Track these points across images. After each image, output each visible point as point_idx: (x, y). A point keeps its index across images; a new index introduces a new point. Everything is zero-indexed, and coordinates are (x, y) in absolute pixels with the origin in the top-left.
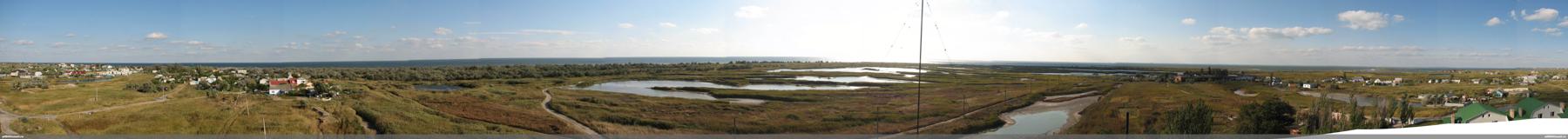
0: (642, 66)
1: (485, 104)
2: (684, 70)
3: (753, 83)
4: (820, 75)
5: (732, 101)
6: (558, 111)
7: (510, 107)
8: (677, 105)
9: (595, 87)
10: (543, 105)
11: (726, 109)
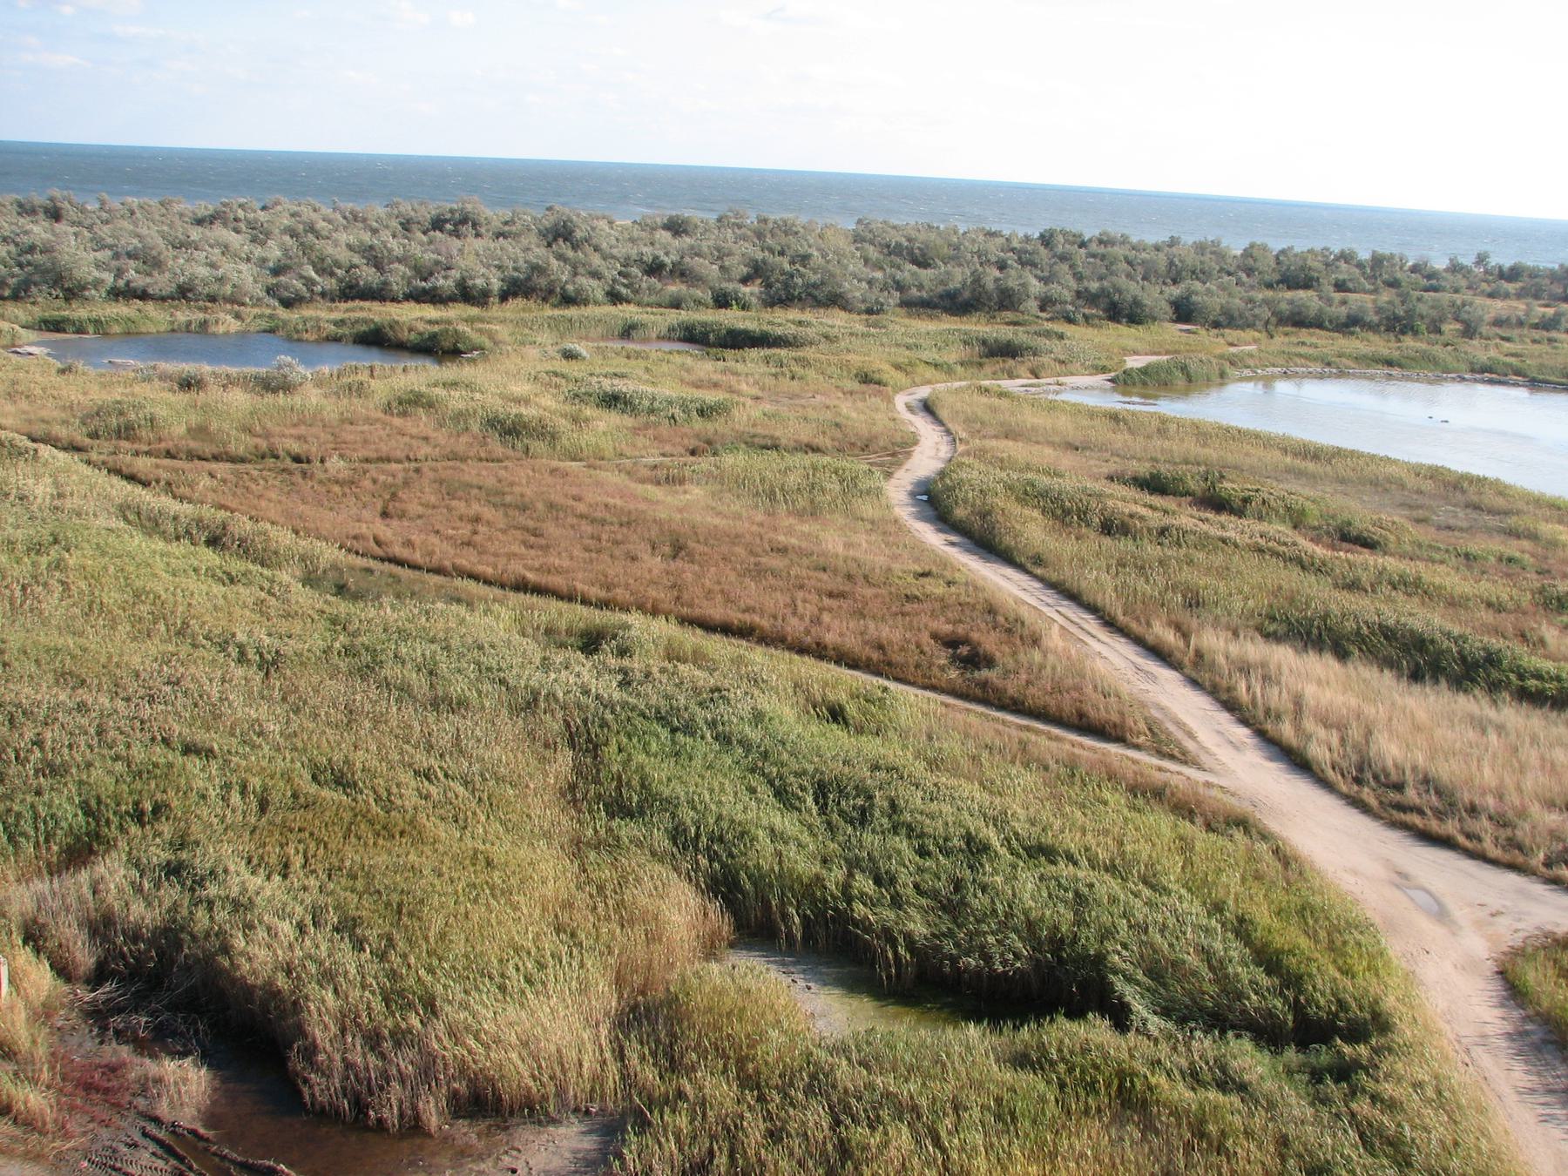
1: (527, 476)
6: (987, 544)
7: (692, 503)
9: (1235, 406)
10: (898, 491)
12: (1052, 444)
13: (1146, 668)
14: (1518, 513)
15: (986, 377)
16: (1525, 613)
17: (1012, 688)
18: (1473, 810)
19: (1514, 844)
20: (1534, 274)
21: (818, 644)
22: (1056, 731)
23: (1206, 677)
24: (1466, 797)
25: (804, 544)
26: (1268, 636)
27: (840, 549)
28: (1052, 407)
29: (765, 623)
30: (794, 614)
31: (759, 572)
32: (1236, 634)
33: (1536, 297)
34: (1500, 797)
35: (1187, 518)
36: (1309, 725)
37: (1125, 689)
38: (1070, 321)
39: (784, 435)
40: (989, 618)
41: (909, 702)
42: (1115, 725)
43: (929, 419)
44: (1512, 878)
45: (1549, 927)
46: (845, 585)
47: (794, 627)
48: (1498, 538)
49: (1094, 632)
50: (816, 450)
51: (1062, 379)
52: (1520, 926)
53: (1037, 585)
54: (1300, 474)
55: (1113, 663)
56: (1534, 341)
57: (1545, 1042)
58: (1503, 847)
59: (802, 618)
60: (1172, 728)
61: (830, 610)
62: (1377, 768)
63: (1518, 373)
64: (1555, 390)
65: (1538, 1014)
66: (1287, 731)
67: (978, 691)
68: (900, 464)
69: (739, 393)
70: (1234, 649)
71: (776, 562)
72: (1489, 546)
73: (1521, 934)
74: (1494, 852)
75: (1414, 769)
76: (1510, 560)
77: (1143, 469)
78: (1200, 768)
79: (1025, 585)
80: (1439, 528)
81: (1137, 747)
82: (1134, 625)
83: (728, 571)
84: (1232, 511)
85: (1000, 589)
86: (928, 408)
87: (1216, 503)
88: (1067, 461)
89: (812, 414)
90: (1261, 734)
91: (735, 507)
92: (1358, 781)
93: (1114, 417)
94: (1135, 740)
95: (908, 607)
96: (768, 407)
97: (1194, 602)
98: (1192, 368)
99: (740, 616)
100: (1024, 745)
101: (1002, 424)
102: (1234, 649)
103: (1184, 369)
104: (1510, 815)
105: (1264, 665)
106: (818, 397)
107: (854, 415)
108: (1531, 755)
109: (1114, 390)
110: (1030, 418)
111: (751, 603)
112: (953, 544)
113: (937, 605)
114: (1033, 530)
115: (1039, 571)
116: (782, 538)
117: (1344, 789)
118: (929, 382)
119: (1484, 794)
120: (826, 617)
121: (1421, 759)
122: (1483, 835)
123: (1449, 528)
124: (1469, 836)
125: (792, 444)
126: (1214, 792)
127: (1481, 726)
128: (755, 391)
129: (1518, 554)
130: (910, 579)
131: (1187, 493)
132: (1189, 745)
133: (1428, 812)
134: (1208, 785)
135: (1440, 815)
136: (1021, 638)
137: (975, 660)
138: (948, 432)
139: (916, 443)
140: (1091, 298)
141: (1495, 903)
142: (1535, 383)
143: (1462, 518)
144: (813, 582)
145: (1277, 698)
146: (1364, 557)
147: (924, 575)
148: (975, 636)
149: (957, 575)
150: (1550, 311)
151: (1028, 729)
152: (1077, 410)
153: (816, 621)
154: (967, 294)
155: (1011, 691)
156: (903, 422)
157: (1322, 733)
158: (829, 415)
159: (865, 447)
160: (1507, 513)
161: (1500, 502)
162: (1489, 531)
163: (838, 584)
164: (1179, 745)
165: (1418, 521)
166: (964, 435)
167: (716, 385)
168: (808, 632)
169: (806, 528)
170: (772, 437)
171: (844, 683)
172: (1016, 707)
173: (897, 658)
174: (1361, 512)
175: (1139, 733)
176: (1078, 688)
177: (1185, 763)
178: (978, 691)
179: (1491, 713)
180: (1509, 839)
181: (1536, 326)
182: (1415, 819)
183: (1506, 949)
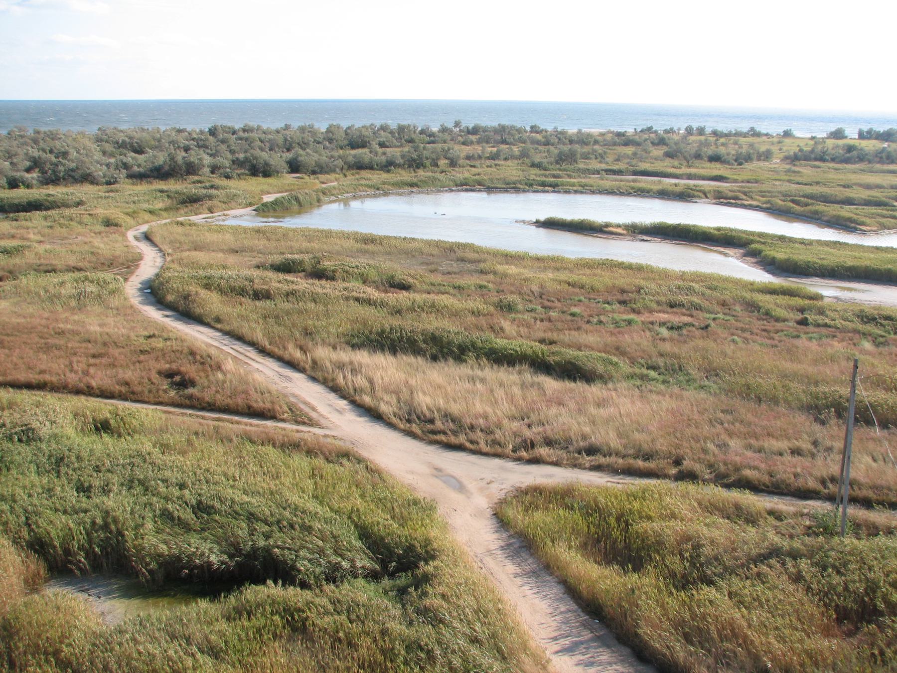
2: (656, 159)
8: (627, 293)
10: (132, 289)
11: (809, 317)
12: (222, 251)
13: (285, 374)
14: (484, 261)
15: (182, 216)
16: (492, 315)
17: (208, 396)
18: (472, 428)
19: (495, 442)
20: (485, 130)
21: (88, 387)
22: (236, 418)
23: (319, 375)
24: (468, 421)
25: (75, 328)
26: (354, 347)
27: (98, 329)
28: (221, 229)
29: (54, 379)
30: (71, 371)
31: (47, 349)
32: (335, 348)
33: (487, 142)
34: (486, 417)
35: (301, 283)
36: (380, 393)
37: (273, 388)
38: (228, 177)
39: (57, 263)
40: (190, 357)
41: (147, 414)
42: (269, 410)
43: (148, 244)
44: (497, 461)
45: (518, 485)
46: (102, 350)
47: (72, 379)
48: (476, 275)
49: (253, 357)
50: (80, 270)
51: (226, 212)
52: (503, 487)
53: (218, 334)
54: (364, 252)
55: (265, 373)
56: (488, 166)
57: (520, 547)
59: (76, 372)
60: (302, 406)
61: (95, 365)
62: (419, 411)
63: (480, 184)
64: (500, 192)
65: (516, 533)
66: (367, 400)
67: (187, 402)
68: (132, 273)
69: (28, 239)
70: (334, 356)
71: (61, 342)
72: (470, 281)
73: (504, 491)
74: (486, 449)
75: (439, 410)
76: (481, 287)
77: (277, 259)
78: (321, 427)
79: (211, 335)
80: (443, 274)
81: (283, 420)
82: (276, 350)
83: (27, 350)
84: (327, 278)
85: (197, 339)
86: (147, 237)
87: (319, 274)
88: (231, 259)
89: (75, 248)
90: (353, 402)
91: (31, 310)
92: (409, 421)
93: (258, 231)
94: (282, 417)
95: (142, 357)
96: (48, 247)
97: (307, 333)
98: (301, 198)
99: (37, 376)
100: (217, 430)
101: (193, 243)
102: (334, 356)
103: (297, 199)
105: (351, 363)
106: (80, 238)
107: (102, 246)
108: (500, 393)
109: (257, 215)
110: (210, 237)
111: (43, 367)
112: (167, 316)
113: (160, 354)
114: (212, 302)
115: (219, 326)
116: (61, 326)
117: (402, 426)
118: (148, 222)
119: (476, 418)
120: (92, 370)
121: (441, 402)
122: (479, 440)
123: (449, 273)
124: (472, 442)
125: (65, 267)
126: (329, 440)
127: (472, 379)
128: (39, 238)
130: (142, 340)
131: (303, 271)
132: (314, 415)
133: (449, 433)
134: (326, 436)
135: (455, 433)
136: (211, 366)
137: (184, 383)
138: (160, 250)
139: (141, 259)
140: (236, 162)
141: (488, 476)
143: (455, 267)
144: (82, 350)
145: (360, 381)
146: (403, 295)
147: (150, 337)
148: (183, 369)
149: (171, 334)
150: (495, 149)
151: (218, 420)
152: (235, 230)
153: (86, 373)
154: (167, 168)
155: (207, 399)
156: (132, 247)
157: (387, 398)
158: (87, 248)
159: (110, 264)
160: (479, 261)
162: (470, 272)
163: (98, 349)
164: (307, 415)
165: (432, 271)
166: (170, 251)
167: (13, 237)
168: (80, 380)
169: (76, 317)
170: (51, 265)
171: (104, 408)
172: (211, 407)
173: (138, 389)
174: (400, 270)
175: (283, 413)
176: (246, 392)
177: (312, 425)
178: (187, 402)
179: (479, 373)
180: (493, 440)
181: (488, 158)
182: (442, 438)
183: (497, 501)
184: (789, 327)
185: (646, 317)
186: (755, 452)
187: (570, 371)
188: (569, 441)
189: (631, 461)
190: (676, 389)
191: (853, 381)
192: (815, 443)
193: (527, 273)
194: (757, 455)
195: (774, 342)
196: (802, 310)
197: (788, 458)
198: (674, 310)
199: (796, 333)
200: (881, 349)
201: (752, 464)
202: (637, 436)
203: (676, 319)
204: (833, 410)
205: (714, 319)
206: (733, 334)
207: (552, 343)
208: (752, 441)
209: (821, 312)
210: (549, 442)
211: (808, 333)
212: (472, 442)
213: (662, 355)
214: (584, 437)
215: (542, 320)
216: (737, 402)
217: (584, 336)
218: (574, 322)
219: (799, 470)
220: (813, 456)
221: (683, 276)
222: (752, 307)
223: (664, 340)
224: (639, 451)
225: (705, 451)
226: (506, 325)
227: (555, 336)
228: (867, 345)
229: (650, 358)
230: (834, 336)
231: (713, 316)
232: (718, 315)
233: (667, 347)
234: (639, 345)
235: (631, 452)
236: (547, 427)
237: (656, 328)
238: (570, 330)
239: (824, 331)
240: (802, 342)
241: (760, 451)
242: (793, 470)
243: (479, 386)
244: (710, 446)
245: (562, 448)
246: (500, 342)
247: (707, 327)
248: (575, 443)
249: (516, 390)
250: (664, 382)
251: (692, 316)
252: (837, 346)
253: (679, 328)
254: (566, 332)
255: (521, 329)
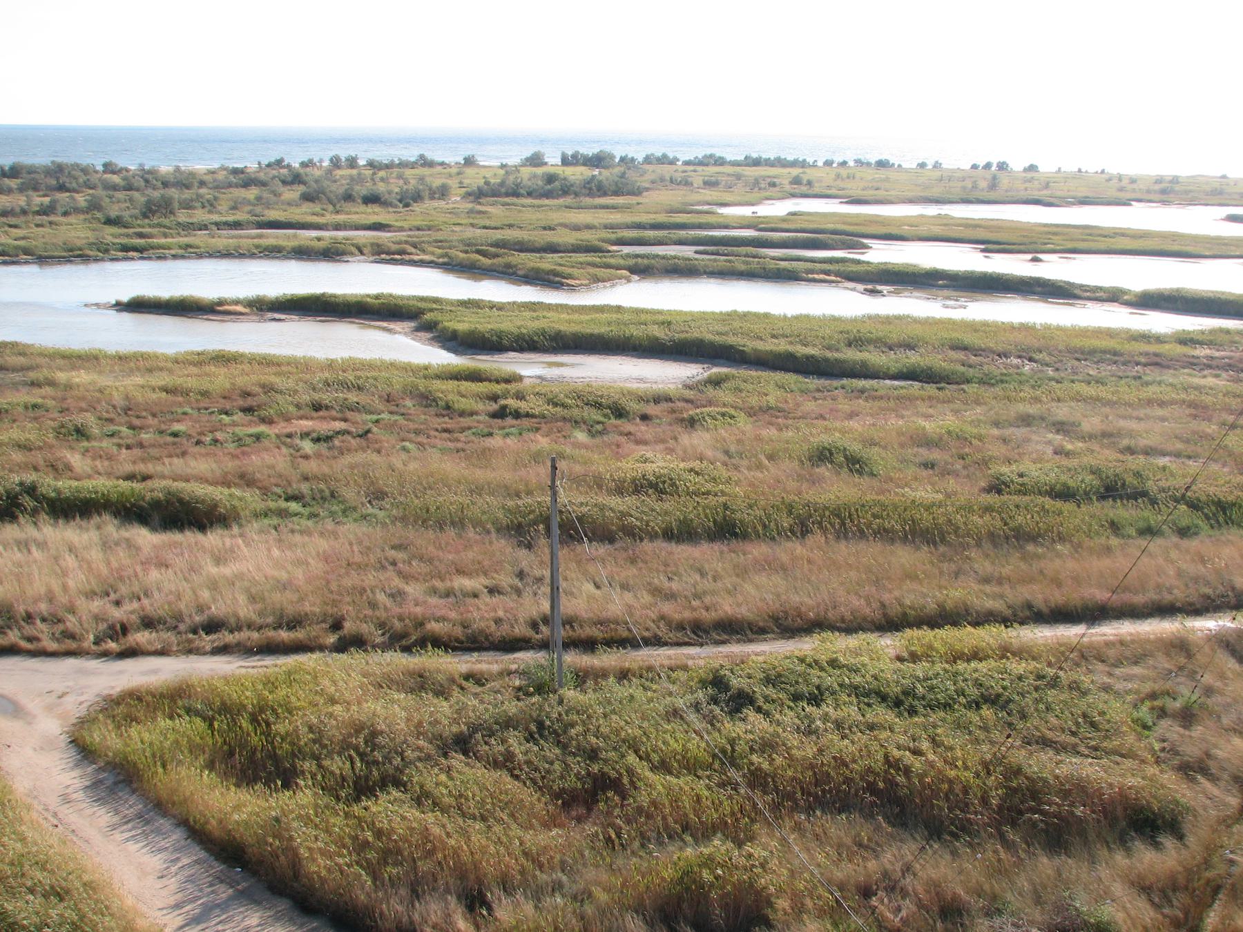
0: (60, 178)
3: (644, 270)
4: (992, 242)
5: (531, 368)
18: (29, 618)
20: (31, 170)
24: (21, 609)
33: (35, 189)
34: (51, 598)
44: (71, 662)
45: (106, 692)
48: (24, 390)
52: (82, 698)
56: (38, 226)
57: (115, 783)
58: (58, 640)
63: (27, 252)
64: (60, 263)
65: (108, 763)
73: (86, 705)
74: (53, 646)
76: (35, 406)
104: (60, 614)
108: (70, 561)
122: (40, 636)
124: (30, 639)
127: (24, 545)
129: (40, 401)
141: (60, 687)
142: (43, 259)
150: (47, 200)
160: (30, 368)
161: (22, 360)
162: (15, 386)
180: (63, 632)
181: (38, 213)
183: (75, 721)
184: (478, 422)
185: (281, 428)
186: (441, 597)
187: (179, 515)
188: (179, 617)
189: (271, 633)
190: (329, 525)
191: (553, 487)
192: (521, 575)
193: (104, 381)
194: (442, 601)
195: (460, 445)
196: (494, 398)
197: (486, 598)
198: (321, 413)
199: (486, 430)
200: (598, 440)
201: (439, 613)
202: (277, 597)
203: (324, 427)
204: (541, 527)
205: (377, 421)
206: (403, 440)
207: (145, 478)
208: (438, 584)
209: (520, 396)
210: (148, 623)
211: (504, 428)
212: (30, 639)
213: (306, 479)
214: (201, 609)
215: (128, 447)
216: (411, 534)
217: (193, 463)
218: (176, 443)
219: (501, 613)
220: (519, 592)
221: (331, 365)
222: (427, 399)
223: (306, 457)
224: (282, 617)
225: (373, 605)
226: (76, 460)
227: (150, 468)
228: (581, 436)
229: (290, 484)
230: (538, 429)
231: (375, 417)
232: (383, 416)
233: (312, 466)
234: (273, 467)
235: (270, 620)
236: (145, 602)
237: (298, 441)
238: (170, 456)
239: (526, 422)
240: (496, 442)
241: (447, 595)
242: (492, 614)
243: (36, 553)
244: (381, 597)
245: (168, 629)
246: (66, 486)
247: (368, 431)
248: (187, 619)
249: (96, 555)
250: (313, 516)
251: (345, 420)
252: (542, 442)
253: (328, 439)
254: (167, 461)
255: (98, 463)
